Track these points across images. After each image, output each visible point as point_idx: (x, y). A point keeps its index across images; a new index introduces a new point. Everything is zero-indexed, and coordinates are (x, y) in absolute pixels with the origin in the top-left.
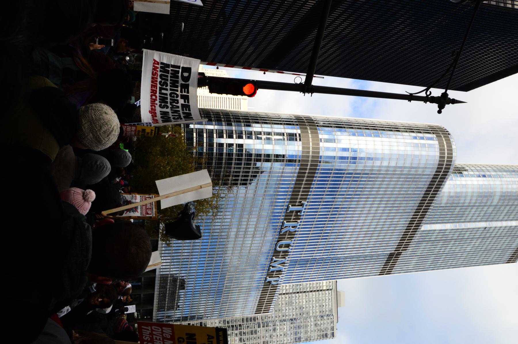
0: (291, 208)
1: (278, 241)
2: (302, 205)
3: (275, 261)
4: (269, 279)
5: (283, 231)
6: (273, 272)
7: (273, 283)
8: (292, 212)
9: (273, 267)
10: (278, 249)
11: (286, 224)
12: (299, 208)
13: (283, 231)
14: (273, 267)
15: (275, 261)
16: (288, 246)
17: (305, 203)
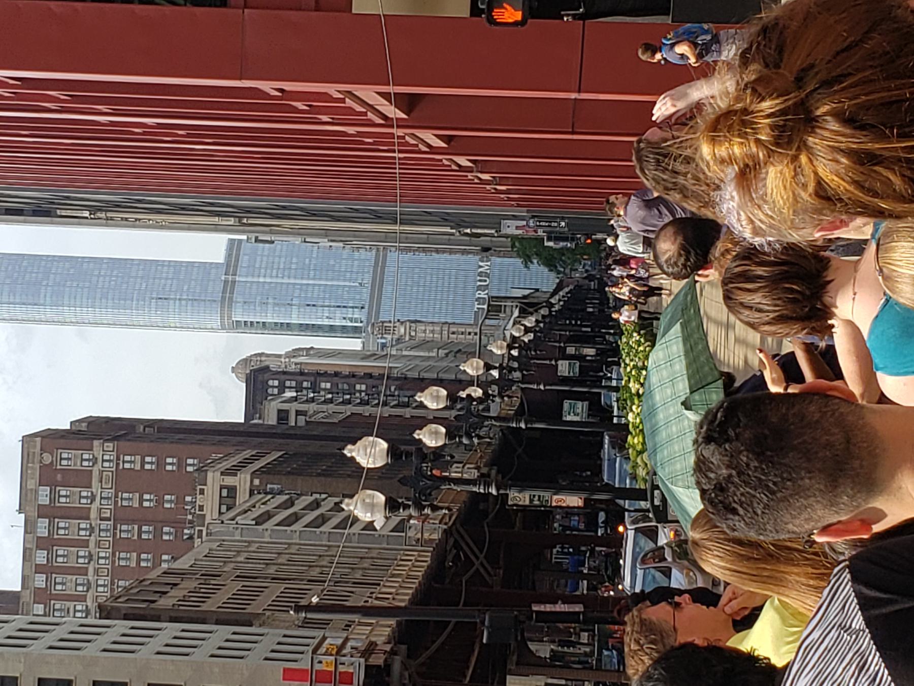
1: (487, 285)
2: (478, 308)
5: (486, 292)
9: (487, 265)
10: (487, 279)
13: (486, 292)
14: (487, 265)
16: (480, 281)
17: (476, 310)
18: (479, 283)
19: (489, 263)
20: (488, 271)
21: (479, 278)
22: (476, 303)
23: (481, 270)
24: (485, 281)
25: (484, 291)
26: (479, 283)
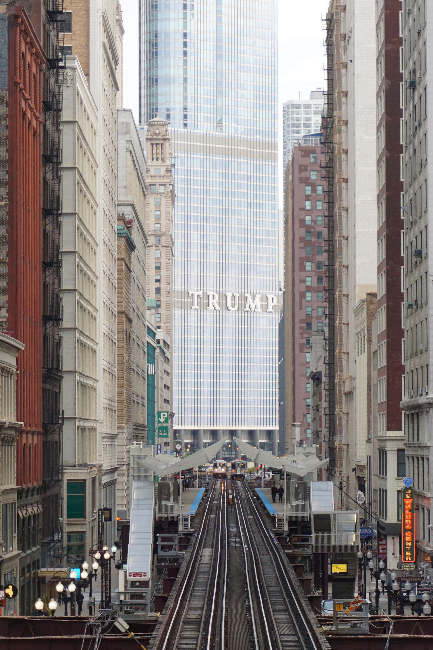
0: (196, 306)
2: (193, 295)
3: (250, 307)
4: (270, 309)
5: (217, 307)
6: (262, 307)
7: (275, 303)
8: (199, 304)
9: (256, 308)
10: (236, 308)
11: (211, 307)
12: (196, 297)
13: (217, 307)
14: (256, 308)
15: (250, 307)
17: (191, 293)
18: (229, 295)
19: (259, 309)
20: (247, 309)
21: (237, 295)
22: (200, 293)
23: (249, 296)
24: (233, 305)
25: (219, 304)
26: (229, 295)
